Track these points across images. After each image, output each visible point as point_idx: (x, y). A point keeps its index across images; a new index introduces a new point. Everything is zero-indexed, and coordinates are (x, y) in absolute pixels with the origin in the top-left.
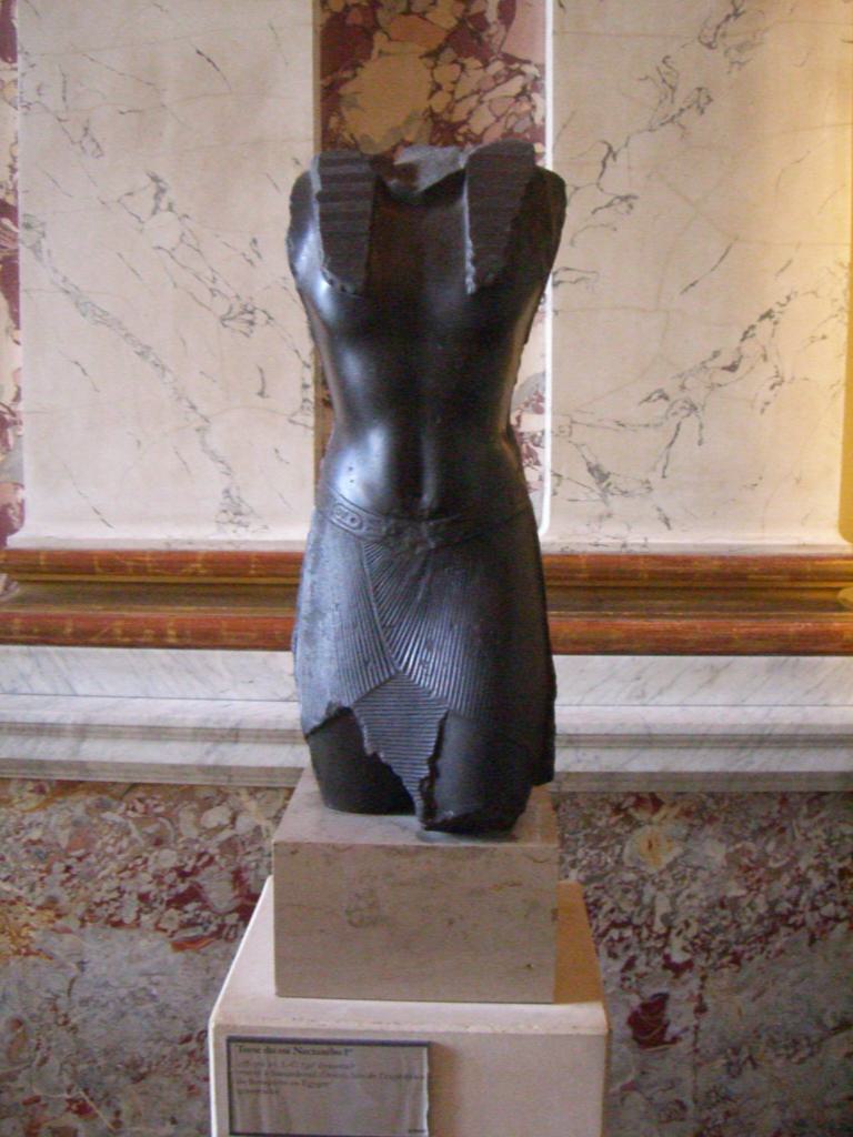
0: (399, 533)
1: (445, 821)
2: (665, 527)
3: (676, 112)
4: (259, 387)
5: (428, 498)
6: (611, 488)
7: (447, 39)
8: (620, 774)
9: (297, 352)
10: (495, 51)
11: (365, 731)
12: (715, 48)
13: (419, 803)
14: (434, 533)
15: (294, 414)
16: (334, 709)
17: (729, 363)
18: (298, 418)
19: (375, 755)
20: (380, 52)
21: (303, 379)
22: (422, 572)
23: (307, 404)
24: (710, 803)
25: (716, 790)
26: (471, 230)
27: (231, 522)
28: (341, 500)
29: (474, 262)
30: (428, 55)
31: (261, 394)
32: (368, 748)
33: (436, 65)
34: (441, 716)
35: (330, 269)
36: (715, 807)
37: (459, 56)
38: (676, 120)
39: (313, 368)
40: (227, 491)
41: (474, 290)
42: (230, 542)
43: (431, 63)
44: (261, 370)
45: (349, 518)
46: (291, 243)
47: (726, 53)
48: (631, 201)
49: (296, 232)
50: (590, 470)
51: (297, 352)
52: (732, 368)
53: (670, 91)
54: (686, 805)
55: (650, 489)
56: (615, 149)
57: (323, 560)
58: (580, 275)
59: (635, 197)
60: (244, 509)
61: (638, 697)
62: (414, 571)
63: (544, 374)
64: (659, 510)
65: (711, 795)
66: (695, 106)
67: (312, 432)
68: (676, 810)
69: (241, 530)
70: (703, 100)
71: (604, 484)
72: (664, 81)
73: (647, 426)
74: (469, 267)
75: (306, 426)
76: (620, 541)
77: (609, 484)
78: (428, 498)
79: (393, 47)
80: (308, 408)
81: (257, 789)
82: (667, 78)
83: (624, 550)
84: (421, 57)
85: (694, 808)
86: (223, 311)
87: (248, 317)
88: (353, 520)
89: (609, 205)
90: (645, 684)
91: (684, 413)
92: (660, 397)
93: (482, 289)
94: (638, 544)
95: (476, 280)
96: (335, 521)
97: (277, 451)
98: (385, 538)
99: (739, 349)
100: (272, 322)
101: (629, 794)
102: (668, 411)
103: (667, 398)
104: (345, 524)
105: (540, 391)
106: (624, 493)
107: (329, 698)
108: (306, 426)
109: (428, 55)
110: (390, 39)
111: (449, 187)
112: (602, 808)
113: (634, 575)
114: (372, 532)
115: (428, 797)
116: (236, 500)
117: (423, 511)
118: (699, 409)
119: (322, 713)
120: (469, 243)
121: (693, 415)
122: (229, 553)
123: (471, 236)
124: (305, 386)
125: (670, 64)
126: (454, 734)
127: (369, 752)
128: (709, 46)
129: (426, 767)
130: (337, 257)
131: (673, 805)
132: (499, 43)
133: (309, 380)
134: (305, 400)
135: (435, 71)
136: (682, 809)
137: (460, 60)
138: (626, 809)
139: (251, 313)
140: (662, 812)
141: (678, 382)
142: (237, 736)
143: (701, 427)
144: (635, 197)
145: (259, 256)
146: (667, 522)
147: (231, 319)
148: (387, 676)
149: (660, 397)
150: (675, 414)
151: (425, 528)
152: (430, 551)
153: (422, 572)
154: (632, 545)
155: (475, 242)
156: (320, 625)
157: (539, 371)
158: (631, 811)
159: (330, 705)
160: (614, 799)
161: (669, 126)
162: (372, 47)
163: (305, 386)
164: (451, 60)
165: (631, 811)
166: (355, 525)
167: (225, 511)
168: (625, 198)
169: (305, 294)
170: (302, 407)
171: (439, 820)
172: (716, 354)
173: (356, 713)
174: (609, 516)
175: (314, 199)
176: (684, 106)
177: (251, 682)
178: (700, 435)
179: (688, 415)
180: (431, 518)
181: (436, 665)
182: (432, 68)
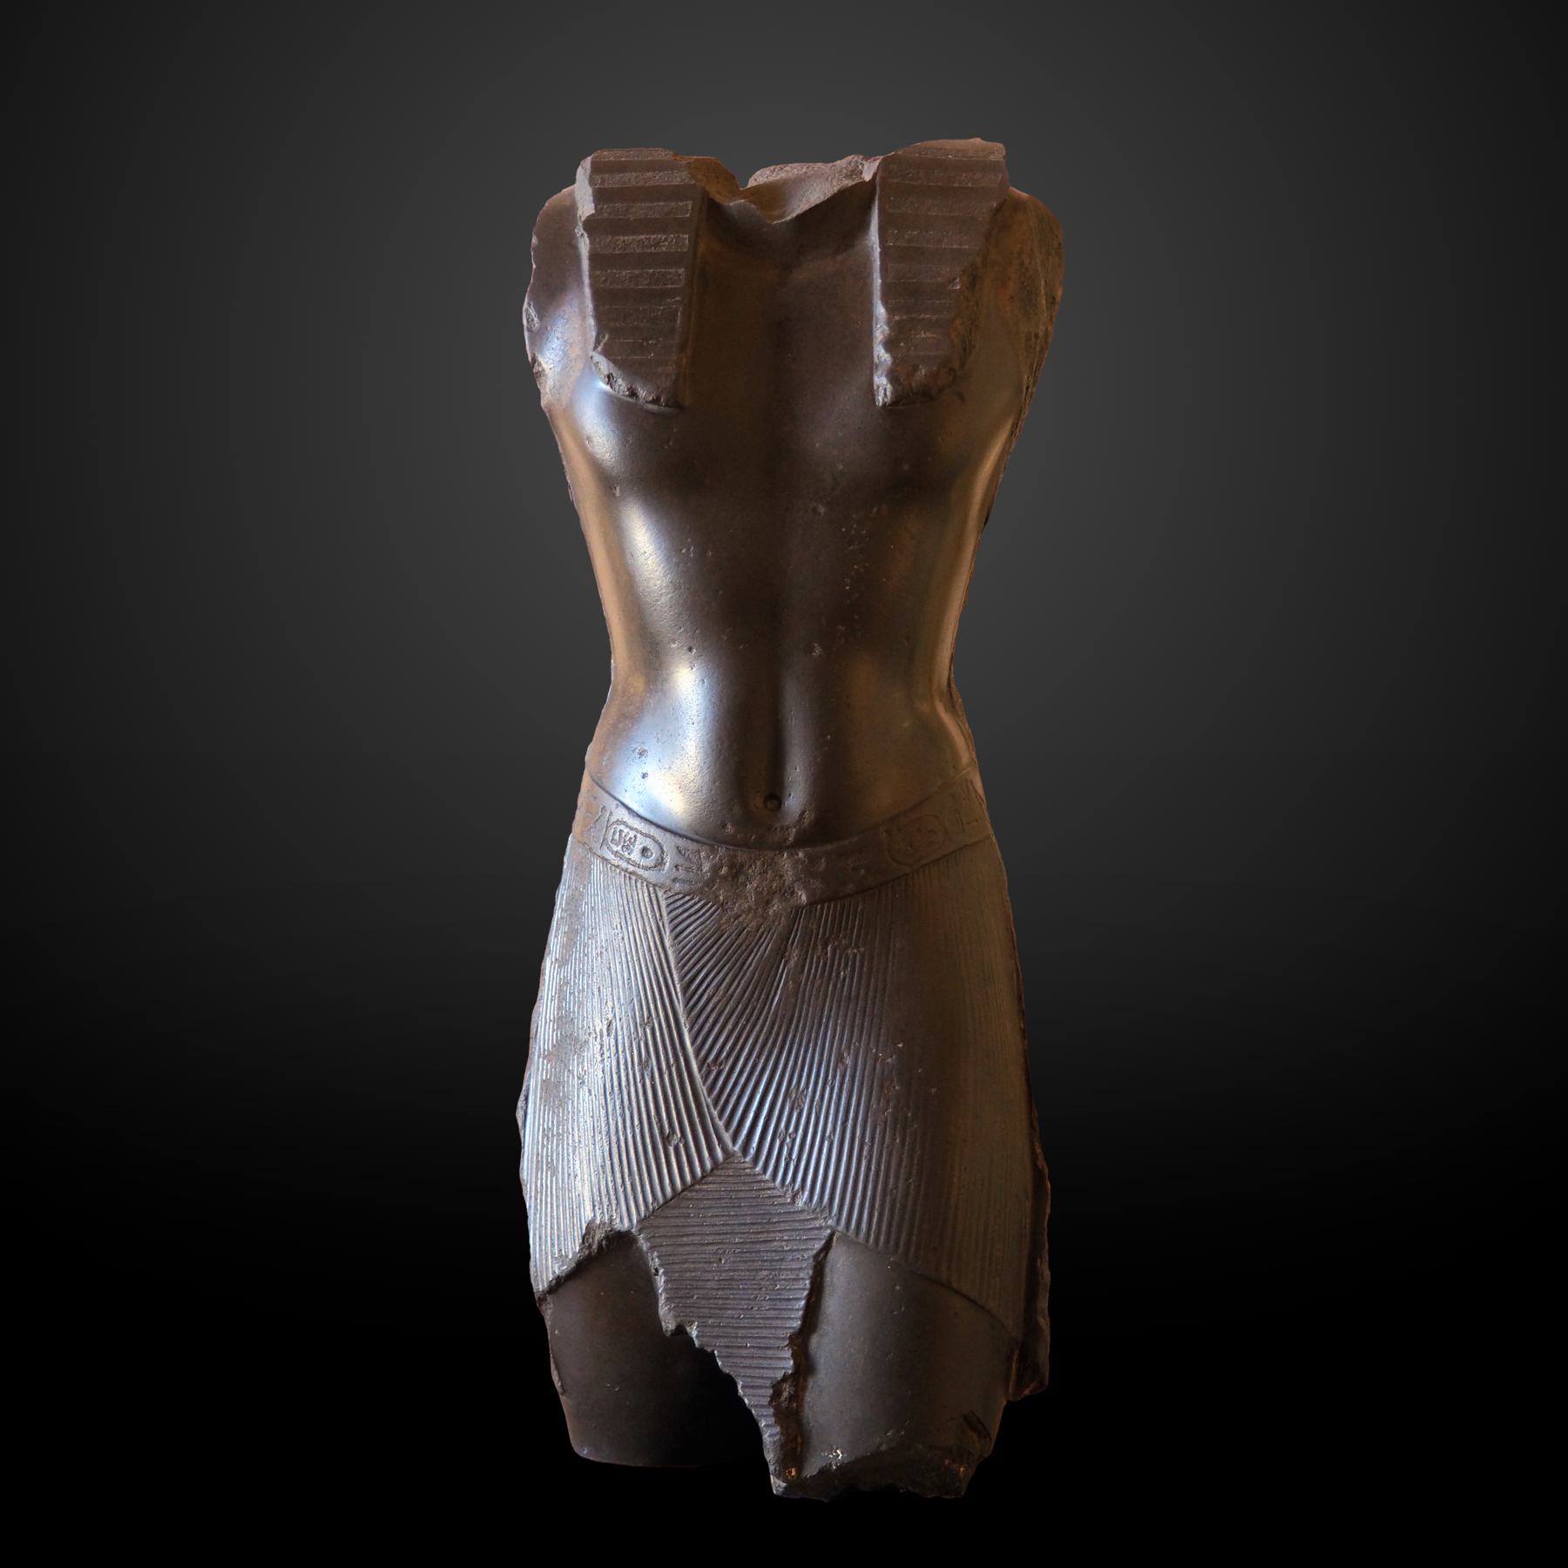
0: (736, 871)
5: (796, 799)
11: (661, 1281)
14: (807, 872)
19: (680, 1330)
22: (781, 953)
26: (884, 285)
29: (890, 345)
32: (668, 1319)
34: (818, 1245)
35: (607, 353)
41: (888, 400)
45: (637, 848)
57: (584, 936)
62: (766, 947)
74: (881, 354)
78: (796, 799)
88: (644, 850)
95: (893, 377)
96: (610, 856)
98: (710, 883)
104: (628, 861)
107: (588, 1214)
114: (682, 873)
115: (791, 1415)
117: (786, 829)
120: (880, 311)
123: (885, 303)
126: (841, 1266)
127: (669, 1324)
129: (788, 1353)
148: (708, 1165)
151: (786, 863)
152: (798, 909)
153: (781, 953)
155: (891, 311)
166: (650, 862)
173: (644, 1244)
175: (579, 230)
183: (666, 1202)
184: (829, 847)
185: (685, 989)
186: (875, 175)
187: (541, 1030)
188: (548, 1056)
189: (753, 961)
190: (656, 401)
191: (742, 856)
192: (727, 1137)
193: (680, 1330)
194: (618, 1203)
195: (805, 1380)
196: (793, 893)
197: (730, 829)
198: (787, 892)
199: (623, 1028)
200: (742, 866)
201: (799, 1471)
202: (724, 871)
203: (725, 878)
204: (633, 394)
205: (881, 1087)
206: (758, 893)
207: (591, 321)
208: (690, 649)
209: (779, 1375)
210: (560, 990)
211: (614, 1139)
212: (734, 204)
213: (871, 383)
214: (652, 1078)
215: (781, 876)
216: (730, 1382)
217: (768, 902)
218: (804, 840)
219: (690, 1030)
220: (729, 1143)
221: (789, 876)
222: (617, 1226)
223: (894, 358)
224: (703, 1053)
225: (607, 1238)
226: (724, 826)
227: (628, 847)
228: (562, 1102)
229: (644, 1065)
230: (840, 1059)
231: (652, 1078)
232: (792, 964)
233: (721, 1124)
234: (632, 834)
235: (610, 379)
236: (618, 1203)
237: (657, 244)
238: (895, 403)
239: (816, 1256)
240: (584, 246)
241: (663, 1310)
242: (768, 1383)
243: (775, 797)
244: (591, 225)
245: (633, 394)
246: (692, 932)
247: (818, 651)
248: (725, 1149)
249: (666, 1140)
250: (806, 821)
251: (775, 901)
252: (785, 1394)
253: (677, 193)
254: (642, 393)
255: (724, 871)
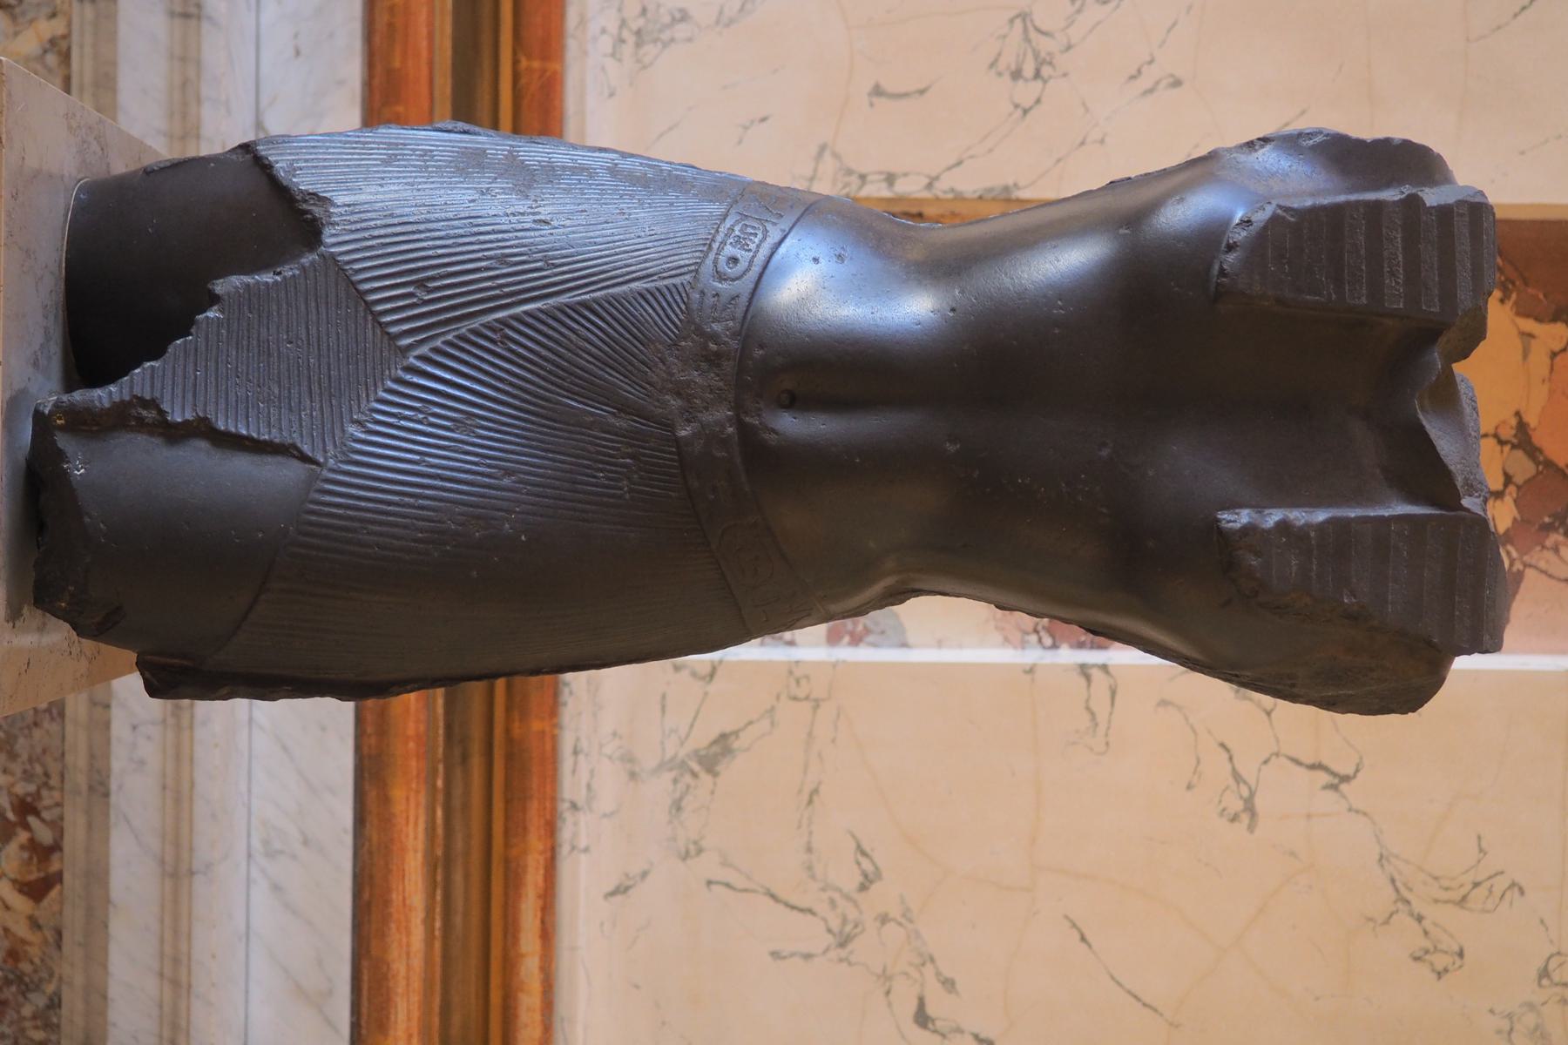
0: (714, 360)
1: (61, 455)
2: (611, 888)
3: (1418, 907)
4: (888, 86)
5: (791, 425)
6: (688, 778)
7: (1549, 464)
8: (107, 815)
9: (959, 163)
10: (1526, 558)
11: (267, 278)
12: (1540, 985)
13: (102, 396)
15: (836, 155)
16: (317, 211)
17: (931, 1010)
18: (828, 165)
19: (214, 299)
20: (1531, 336)
21: (906, 175)
22: (623, 408)
23: (854, 179)
24: (39, 1000)
25: (65, 1011)
26: (1349, 521)
27: (623, 23)
28: (774, 235)
29: (1283, 526)
30: (1522, 426)
31: (878, 91)
33: (1501, 443)
34: (306, 449)
35: (1274, 219)
36: (27, 1011)
37: (1519, 488)
38: (1400, 905)
39: (926, 195)
40: (683, 16)
41: (1224, 525)
42: (583, 21)
43: (1508, 433)
44: (922, 92)
45: (738, 253)
46: (1319, 139)
47: (1531, 1006)
48: (1245, 818)
49: (1342, 153)
50: (723, 737)
51: (959, 163)
52: (922, 1018)
53: (1457, 896)
54: (34, 952)
55: (686, 856)
56: (1344, 787)
58: (1102, 717)
59: (1251, 828)
60: (650, 50)
61: (266, 843)
62: (629, 392)
63: (904, 645)
64: (644, 875)
65: (55, 1003)
66: (1428, 944)
67: (800, 185)
68: (22, 930)
69: (606, 43)
70: (1441, 961)
71: (696, 767)
72: (1476, 885)
73: (809, 850)
74: (1273, 517)
75: (812, 179)
76: (581, 802)
77: (695, 775)
78: (791, 425)
79: (1539, 358)
80: (846, 185)
81: (66, 57)
82: (1481, 892)
83: (564, 806)
84: (1517, 414)
85: (25, 967)
86: (1041, 19)
87: (1029, 70)
88: (734, 260)
89: (1237, 777)
90: (294, 857)
91: (835, 924)
92: (866, 876)
93: (1225, 541)
94: (575, 835)
95: (1249, 530)
96: (728, 223)
97: (763, 120)
98: (699, 331)
99: (959, 1030)
100: (1019, 111)
101: (57, 826)
102: (839, 890)
103: (863, 888)
104: (723, 243)
105: (870, 638)
106: (677, 806)
107: (340, 199)
108: (812, 179)
109: (1522, 426)
110: (1554, 355)
111: (1428, 477)
112: (28, 776)
113: (515, 828)
114: (710, 301)
115: (122, 418)
116: (665, 36)
118: (843, 953)
119: (303, 182)
120: (1321, 516)
121: (830, 939)
122: (562, 16)
124: (890, 179)
125: (1508, 895)
126: (281, 474)
128: (1544, 973)
129: (189, 416)
130: (1297, 237)
131: (35, 924)
132: (1542, 565)
133: (904, 187)
134: (863, 177)
135: (1492, 441)
136: (24, 942)
137: (1512, 489)
138: (27, 827)
139: (1037, 75)
140: (20, 903)
141: (895, 912)
142: (186, 16)
143: (808, 957)
144: (1251, 828)
145: (1150, 91)
146: (620, 890)
147: (1025, 30)
148: (394, 330)
149: (866, 876)
150: (833, 903)
151: (722, 413)
152: (670, 427)
153: (623, 408)
154: (575, 824)
155: (1321, 527)
156: (501, 184)
157: (911, 638)
158: (23, 836)
159: (325, 201)
160: (48, 799)
161: (1389, 891)
162: (1538, 319)
163: (890, 179)
164: (1511, 472)
165: (23, 836)
166: (723, 266)
167: (644, 11)
168: (1250, 807)
169: (1203, 168)
170: (850, 172)
171: (63, 441)
172: (949, 984)
173: (308, 259)
174: (633, 775)
175: (1408, 190)
176: (1427, 923)
177: (298, 53)
178: (792, 955)
179: (829, 931)
180: (745, 431)
181: (412, 446)
182: (1496, 436)
183: (353, 284)
184: (738, 460)
185: (584, 304)
186: (1467, 510)
187: (540, 148)
188: (512, 156)
189: (615, 378)
190: (1222, 272)
191: (729, 366)
192: (424, 350)
193: (214, 299)
194: (352, 231)
195: (160, 435)
196: (689, 421)
197: (759, 353)
198: (689, 415)
199: (542, 237)
200: (718, 366)
201: (61, 428)
202: (713, 346)
203: (705, 347)
204: (1231, 248)
205: (479, 517)
206: (688, 384)
207: (1309, 203)
208: (953, 310)
209: (165, 407)
210: (582, 169)
211: (422, 227)
212: (1436, 357)
213: (1241, 506)
214: (487, 269)
215: (706, 408)
216: (157, 353)
217: (678, 394)
218: (745, 431)
219: (540, 310)
220: (417, 352)
221: (706, 417)
222: (327, 231)
223: (1269, 531)
224: (515, 324)
225: (315, 219)
226: (761, 346)
227: (740, 243)
228: (462, 171)
229: (503, 260)
230: (508, 472)
231: (487, 269)
232: (612, 420)
233: (438, 343)
234: (753, 246)
235: (1246, 222)
236: (352, 231)
237: (1393, 274)
238: (1220, 531)
239: (294, 446)
240: (1391, 195)
241: (236, 281)
242: (157, 395)
243: (793, 402)
244: (1413, 202)
245: (1231, 248)
246: (647, 312)
247: (951, 448)
248: (410, 347)
249: (420, 284)
250: (766, 436)
251: (680, 402)
252: (145, 413)
253: (1448, 296)
254: (1231, 257)
255: (713, 346)
